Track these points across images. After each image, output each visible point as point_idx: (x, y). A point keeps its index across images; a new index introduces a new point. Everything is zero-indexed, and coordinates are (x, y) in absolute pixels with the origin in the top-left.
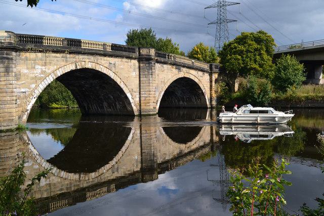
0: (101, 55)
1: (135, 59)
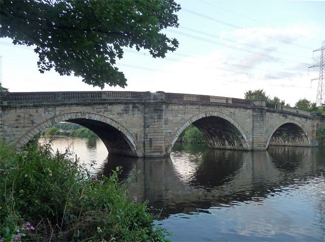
0: (223, 106)
1: (249, 109)
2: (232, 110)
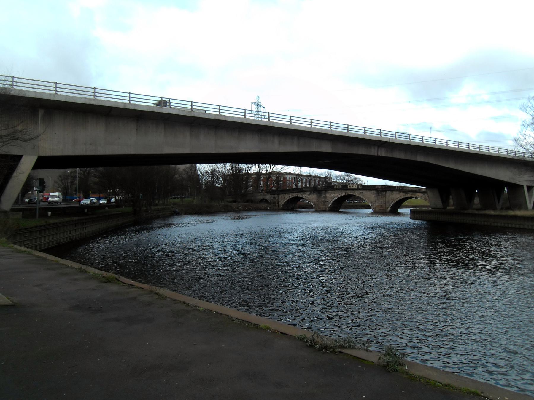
0: (355, 189)
2: (361, 191)
